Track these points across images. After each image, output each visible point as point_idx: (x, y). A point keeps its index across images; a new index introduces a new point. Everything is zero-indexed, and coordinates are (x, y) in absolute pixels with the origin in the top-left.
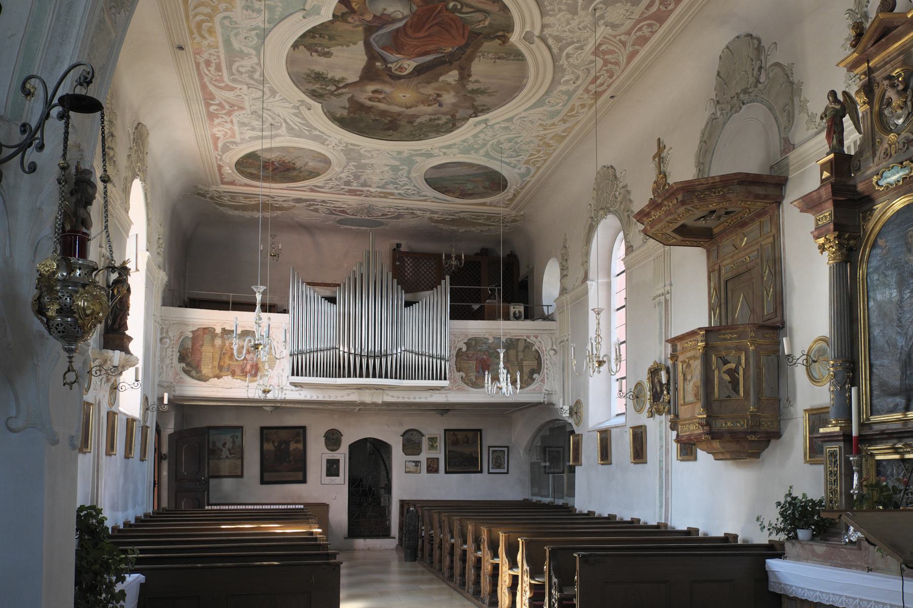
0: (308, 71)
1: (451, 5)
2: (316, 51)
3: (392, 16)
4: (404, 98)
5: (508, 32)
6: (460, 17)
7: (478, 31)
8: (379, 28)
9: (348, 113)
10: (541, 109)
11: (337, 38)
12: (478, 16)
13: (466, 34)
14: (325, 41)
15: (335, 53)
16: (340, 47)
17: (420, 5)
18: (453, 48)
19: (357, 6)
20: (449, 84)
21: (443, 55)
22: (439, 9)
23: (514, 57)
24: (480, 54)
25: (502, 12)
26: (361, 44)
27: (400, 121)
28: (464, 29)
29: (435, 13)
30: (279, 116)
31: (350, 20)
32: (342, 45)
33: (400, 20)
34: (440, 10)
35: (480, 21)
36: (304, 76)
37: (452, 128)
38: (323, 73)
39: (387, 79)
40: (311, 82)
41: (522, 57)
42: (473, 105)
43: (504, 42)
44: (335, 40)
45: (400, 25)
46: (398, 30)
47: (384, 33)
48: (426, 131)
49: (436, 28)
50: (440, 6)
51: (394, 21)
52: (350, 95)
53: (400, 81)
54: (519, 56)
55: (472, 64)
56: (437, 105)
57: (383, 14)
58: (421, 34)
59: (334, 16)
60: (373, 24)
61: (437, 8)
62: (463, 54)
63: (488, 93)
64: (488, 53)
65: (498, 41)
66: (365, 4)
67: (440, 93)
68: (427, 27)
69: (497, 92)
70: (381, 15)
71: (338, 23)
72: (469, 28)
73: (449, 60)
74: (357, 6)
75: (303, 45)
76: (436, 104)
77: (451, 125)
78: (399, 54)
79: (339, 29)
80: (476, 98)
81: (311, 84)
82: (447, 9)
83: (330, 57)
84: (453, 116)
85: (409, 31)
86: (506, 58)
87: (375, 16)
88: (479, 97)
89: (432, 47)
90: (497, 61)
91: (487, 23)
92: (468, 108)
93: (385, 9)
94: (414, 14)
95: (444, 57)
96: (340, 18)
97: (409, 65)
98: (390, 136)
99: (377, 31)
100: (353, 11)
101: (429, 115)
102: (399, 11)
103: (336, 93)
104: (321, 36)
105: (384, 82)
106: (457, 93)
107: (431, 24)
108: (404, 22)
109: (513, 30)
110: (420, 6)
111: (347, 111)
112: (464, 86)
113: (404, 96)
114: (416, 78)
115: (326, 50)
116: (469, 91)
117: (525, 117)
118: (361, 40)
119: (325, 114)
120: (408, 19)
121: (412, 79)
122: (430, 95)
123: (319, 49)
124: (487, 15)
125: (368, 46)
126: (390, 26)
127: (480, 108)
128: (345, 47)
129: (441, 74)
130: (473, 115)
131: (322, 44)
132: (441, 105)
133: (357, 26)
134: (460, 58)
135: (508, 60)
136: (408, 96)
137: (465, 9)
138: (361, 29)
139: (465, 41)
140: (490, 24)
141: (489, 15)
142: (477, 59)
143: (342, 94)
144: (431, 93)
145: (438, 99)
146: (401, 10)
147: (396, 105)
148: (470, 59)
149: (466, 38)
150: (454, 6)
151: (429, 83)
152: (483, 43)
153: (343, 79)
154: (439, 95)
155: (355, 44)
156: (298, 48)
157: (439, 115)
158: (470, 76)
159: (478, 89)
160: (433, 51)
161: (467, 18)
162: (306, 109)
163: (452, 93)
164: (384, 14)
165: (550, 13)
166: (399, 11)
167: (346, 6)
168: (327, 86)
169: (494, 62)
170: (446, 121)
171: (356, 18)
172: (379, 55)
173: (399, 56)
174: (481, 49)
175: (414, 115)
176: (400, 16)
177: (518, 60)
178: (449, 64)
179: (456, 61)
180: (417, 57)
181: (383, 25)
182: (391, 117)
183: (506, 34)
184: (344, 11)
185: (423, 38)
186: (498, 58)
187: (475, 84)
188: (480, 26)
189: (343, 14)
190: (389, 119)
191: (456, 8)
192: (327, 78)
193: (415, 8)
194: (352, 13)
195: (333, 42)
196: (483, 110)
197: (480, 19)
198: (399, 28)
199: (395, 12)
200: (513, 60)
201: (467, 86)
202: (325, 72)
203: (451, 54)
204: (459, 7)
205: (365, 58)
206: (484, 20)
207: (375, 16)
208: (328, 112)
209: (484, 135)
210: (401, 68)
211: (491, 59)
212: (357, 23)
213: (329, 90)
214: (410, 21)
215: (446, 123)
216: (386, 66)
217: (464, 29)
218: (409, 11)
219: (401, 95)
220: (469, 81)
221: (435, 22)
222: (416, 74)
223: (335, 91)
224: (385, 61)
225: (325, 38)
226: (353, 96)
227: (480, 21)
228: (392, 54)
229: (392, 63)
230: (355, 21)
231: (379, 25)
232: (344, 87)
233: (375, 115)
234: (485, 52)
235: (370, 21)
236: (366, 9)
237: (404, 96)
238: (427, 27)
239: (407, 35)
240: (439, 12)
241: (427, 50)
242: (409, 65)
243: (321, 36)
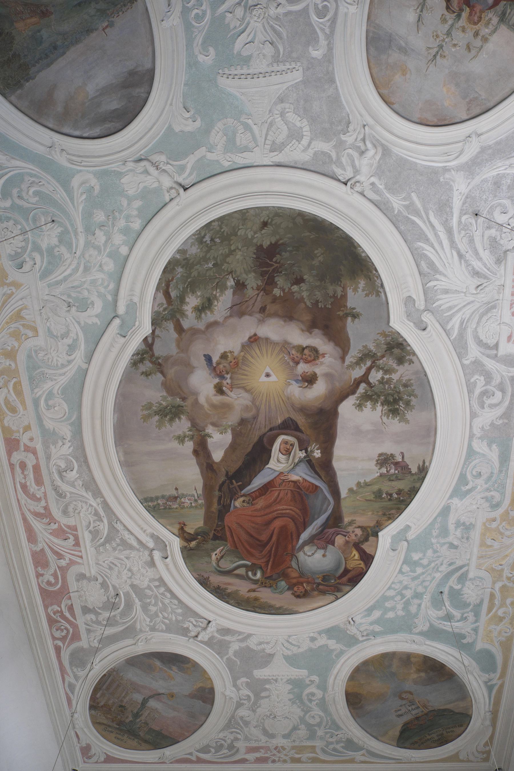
0: (409, 415)
1: (259, 575)
2: (396, 464)
3: (315, 548)
4: (268, 370)
5: (186, 547)
6: (244, 560)
7: (217, 542)
8: (325, 525)
9: (344, 296)
10: (63, 380)
11: (372, 497)
12: (227, 565)
13: (228, 534)
14: (387, 487)
15: (372, 465)
16: (368, 480)
17: (290, 570)
18: (235, 507)
19: (353, 555)
20: (214, 424)
21: (243, 492)
22: (269, 567)
23: (159, 504)
24: (200, 502)
25: (206, 575)
26: (344, 493)
27: (258, 289)
28: (234, 541)
29: (271, 560)
30: (461, 256)
31: (359, 532)
32: (367, 485)
33: (305, 543)
34: (268, 566)
35: (222, 557)
36: (414, 401)
37: (168, 286)
38: (388, 417)
39: (301, 420)
40: (405, 386)
41: (149, 506)
42: (162, 373)
43: (182, 529)
44: (374, 493)
45: (305, 536)
46: (305, 526)
47: (318, 517)
48: (206, 260)
49: (264, 537)
50: (269, 570)
51: (311, 541)
52: (349, 359)
53: (283, 419)
54: (154, 507)
55: (202, 481)
56: (215, 359)
57: (325, 548)
58: (277, 524)
59: (377, 536)
60: (332, 530)
61: (272, 567)
62: (220, 498)
63: (156, 413)
64: (191, 507)
65: (190, 529)
66: (345, 559)
67: (220, 398)
68: (274, 538)
69: (146, 418)
70: (327, 546)
71: (372, 524)
72: (229, 545)
73: (232, 484)
74: (353, 555)
75: (413, 475)
76: (218, 364)
77: (173, 294)
78: (295, 482)
79: (370, 513)
80: (165, 394)
81: (404, 379)
82: (261, 568)
83: (380, 455)
84: (179, 329)
85: (292, 526)
86: (167, 500)
87: (333, 544)
88: (164, 398)
89: (261, 503)
90: (174, 493)
91: (214, 557)
92: (167, 359)
93: (324, 556)
94: (293, 555)
95: (242, 488)
96: (370, 532)
97: (278, 461)
98: (265, 224)
99: (328, 519)
100: (357, 546)
101: (215, 324)
102: (309, 556)
103: (369, 363)
104: (391, 495)
105: (303, 410)
106: (196, 401)
107: (271, 543)
108: (301, 541)
109: (182, 552)
110: (289, 567)
111: (349, 304)
112: (194, 425)
113: (268, 375)
114: (264, 431)
115: (384, 470)
116: (183, 413)
117: (72, 348)
118: (345, 498)
119: (382, 285)
120: (297, 547)
121: (267, 429)
122: (232, 387)
123: (392, 471)
124: (219, 569)
125: (335, 492)
126: (314, 532)
127: (147, 365)
128: (362, 481)
129: (233, 447)
130: (150, 340)
131: (390, 480)
132: (208, 359)
133: (351, 523)
134: (220, 490)
135: (163, 497)
136: (263, 379)
137: (242, 571)
138: (346, 520)
139: (226, 523)
140: (210, 556)
141: (216, 569)
142: (200, 492)
143: (361, 360)
144: (231, 394)
145: (217, 380)
146: (306, 557)
147: (275, 344)
148: (208, 488)
149: (227, 529)
150: (255, 574)
151: (243, 422)
152: (205, 523)
153: (360, 406)
154: (219, 390)
155: (351, 490)
156: (419, 468)
157: (201, 326)
158: (196, 452)
159: (172, 420)
160: (257, 497)
161: (236, 559)
162: (414, 297)
163: (202, 400)
164: (323, 548)
165: (157, 583)
166: (309, 556)
167: (364, 552)
168: (382, 381)
169: (176, 489)
170: (185, 307)
171: (353, 537)
172: (316, 473)
173: (294, 477)
174: (201, 513)
175: (241, 314)
176: (306, 548)
177: (151, 500)
178: (230, 474)
179: (223, 483)
180: (273, 480)
181: (322, 531)
182: (275, 300)
183: (186, 544)
184: (366, 543)
185: (275, 518)
186: (176, 498)
187: (180, 433)
188: (218, 550)
189: (366, 540)
190: (277, 292)
191: (252, 571)
192: (382, 404)
193: (294, 564)
194: (358, 544)
195: (376, 488)
196: (142, 360)
197: (222, 561)
198: (305, 530)
199: (313, 554)
200: (157, 498)
201: (189, 424)
202: (385, 419)
203: (233, 495)
204: (250, 573)
205: (336, 464)
206: (218, 561)
207: (333, 544)
208: (378, 294)
209: (106, 268)
210: (288, 452)
211: (184, 496)
212: (350, 529)
213: (379, 368)
214: (294, 543)
215: (182, 299)
216: (306, 452)
217: (234, 541)
218: (299, 559)
219: (273, 378)
220: (192, 438)
221: (268, 548)
222: (265, 440)
223: (369, 370)
224: (309, 461)
225: (387, 494)
226: (343, 359)
227: (222, 557)
228: (303, 479)
229: (300, 461)
230: (353, 532)
231: (326, 530)
232: (357, 383)
233: (302, 300)
234: (196, 507)
235: (338, 534)
236: (343, 552)
237: (268, 375)
238: (274, 538)
239: (293, 519)
240: (267, 562)
241: (263, 497)
242: (278, 461)
243: (391, 495)
